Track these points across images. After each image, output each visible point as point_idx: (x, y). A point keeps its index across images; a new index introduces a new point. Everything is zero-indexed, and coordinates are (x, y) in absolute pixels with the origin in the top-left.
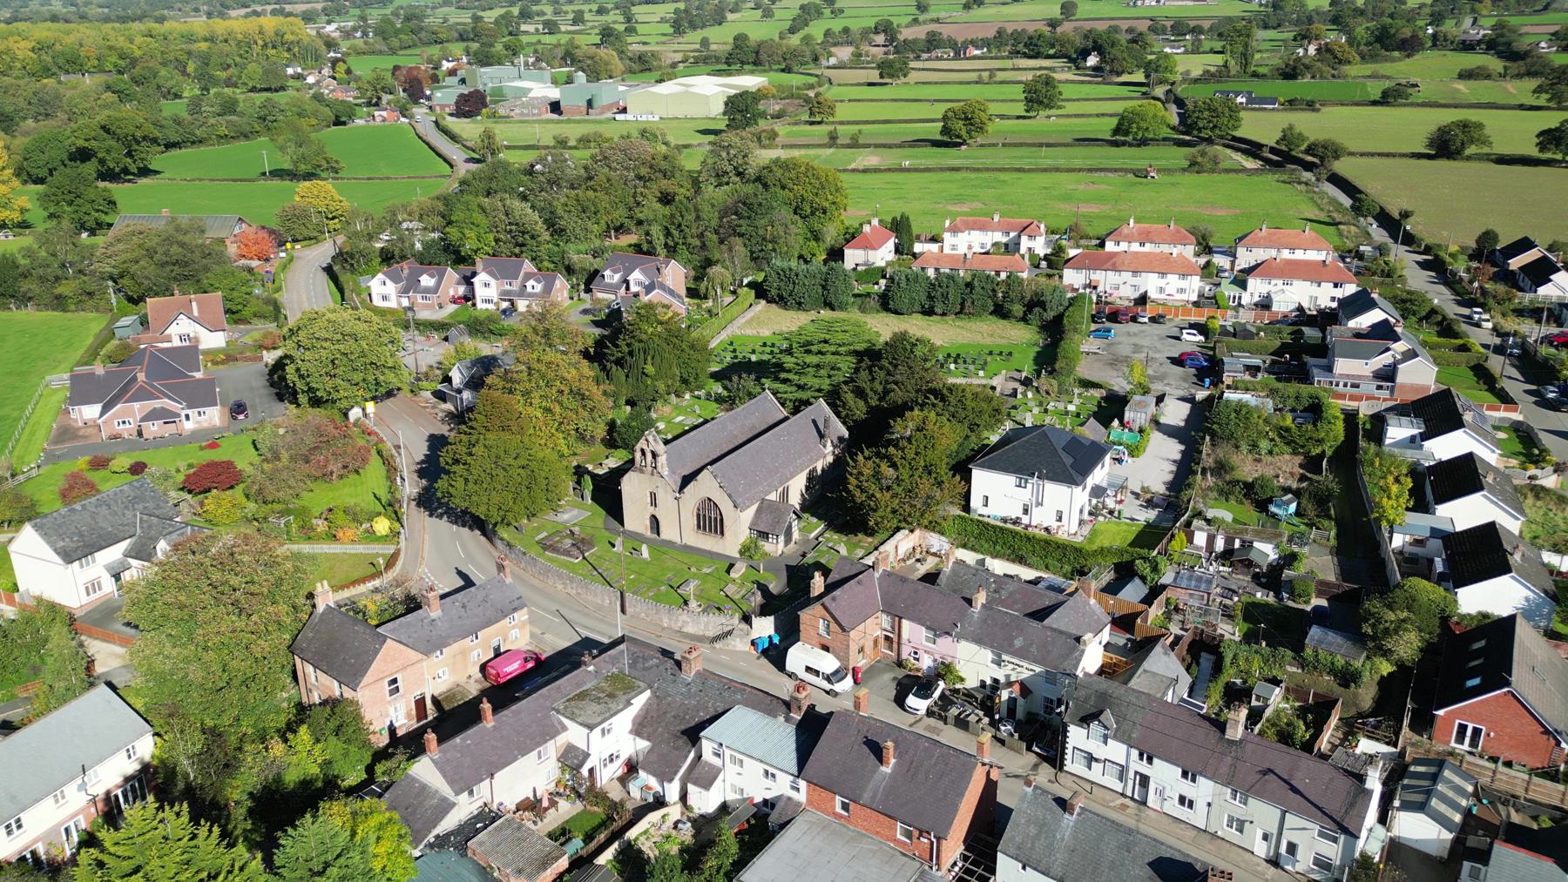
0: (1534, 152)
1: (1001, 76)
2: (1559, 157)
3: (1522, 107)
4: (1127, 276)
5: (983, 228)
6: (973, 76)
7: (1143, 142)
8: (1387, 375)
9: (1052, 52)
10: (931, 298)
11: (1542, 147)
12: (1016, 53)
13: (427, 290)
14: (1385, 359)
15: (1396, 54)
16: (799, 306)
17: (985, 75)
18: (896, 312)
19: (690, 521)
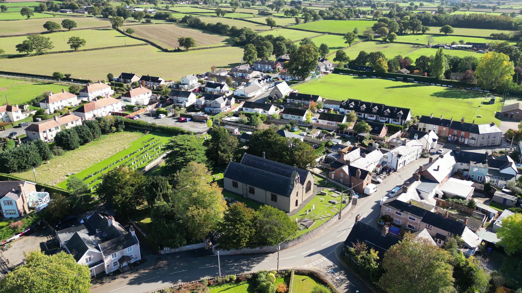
0: (18, 53)
2: (26, 53)
4: (103, 109)
10: (80, 137)
16: (34, 165)
18: (74, 149)
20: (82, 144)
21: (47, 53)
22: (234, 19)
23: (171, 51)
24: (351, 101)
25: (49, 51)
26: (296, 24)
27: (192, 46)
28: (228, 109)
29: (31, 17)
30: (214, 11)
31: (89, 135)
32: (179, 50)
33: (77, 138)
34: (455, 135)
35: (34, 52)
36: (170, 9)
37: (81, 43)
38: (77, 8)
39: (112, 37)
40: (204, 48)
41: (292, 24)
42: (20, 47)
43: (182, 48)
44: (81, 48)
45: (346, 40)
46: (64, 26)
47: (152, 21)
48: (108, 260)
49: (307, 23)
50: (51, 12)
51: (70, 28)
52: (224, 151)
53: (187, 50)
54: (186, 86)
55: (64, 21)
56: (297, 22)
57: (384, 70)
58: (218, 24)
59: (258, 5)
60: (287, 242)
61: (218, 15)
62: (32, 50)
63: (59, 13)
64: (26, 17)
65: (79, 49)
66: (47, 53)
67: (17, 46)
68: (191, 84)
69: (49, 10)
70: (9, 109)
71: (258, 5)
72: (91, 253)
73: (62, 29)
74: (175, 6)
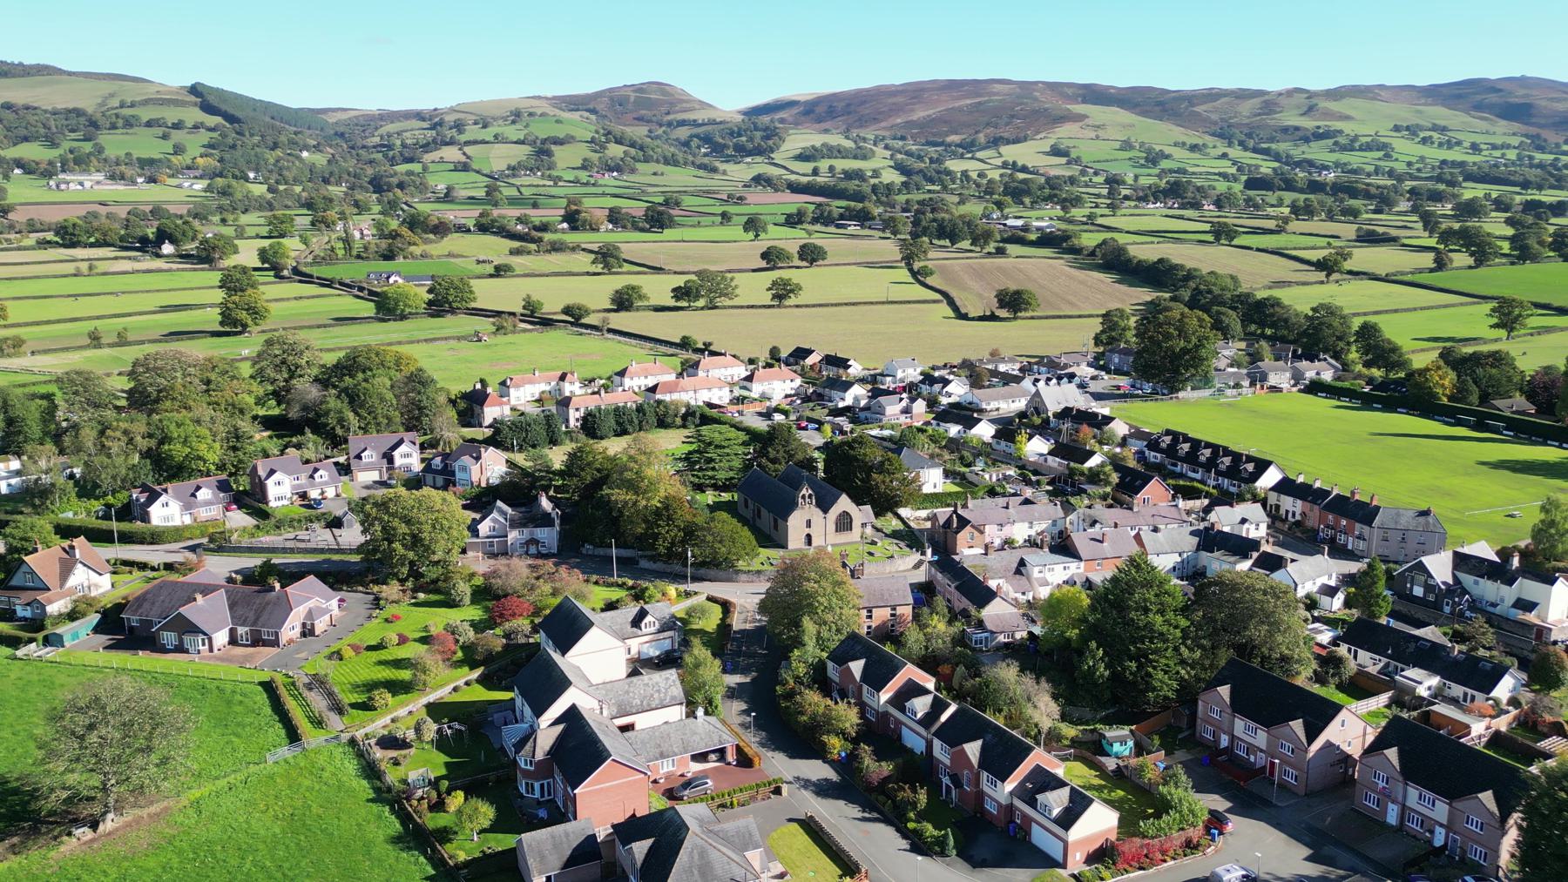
0: (672, 303)
1: (102, 266)
3: (588, 274)
5: (531, 382)
6: (70, 268)
7: (403, 317)
8: (906, 411)
9: (92, 240)
10: (618, 423)
11: (677, 298)
12: (44, 244)
13: (208, 503)
14: (904, 403)
15: (431, 236)
17: (84, 266)
19: (831, 526)
20: (617, 435)
21: (725, 307)
22: (1258, 250)
23: (973, 319)
24: (1168, 432)
25: (728, 302)
26: (1432, 270)
27: (1026, 310)
28: (903, 419)
29: (763, 236)
30: (1207, 227)
31: (631, 422)
32: (993, 318)
33: (612, 422)
34: (1328, 526)
35: (701, 303)
36: (1100, 221)
37: (792, 291)
38: (873, 218)
39: (896, 281)
40: (1060, 317)
41: (1421, 271)
42: (679, 293)
43: (1003, 313)
44: (792, 301)
45: (1495, 320)
46: (801, 258)
47: (1012, 249)
48: (513, 535)
49: (1482, 271)
50: (818, 227)
51: (812, 261)
52: (774, 461)
53: (1015, 318)
54: (889, 379)
55: (803, 247)
56: (1440, 265)
57: (1435, 396)
58: (1161, 261)
59: (1399, 213)
60: (738, 572)
61: (1218, 239)
62: (697, 297)
63: (832, 229)
64: (751, 235)
65: (787, 302)
66: (725, 307)
67: (674, 290)
68: (900, 375)
69: (815, 221)
70: (563, 378)
71: (1399, 213)
72: (495, 520)
73: (797, 262)
74: (1119, 212)
